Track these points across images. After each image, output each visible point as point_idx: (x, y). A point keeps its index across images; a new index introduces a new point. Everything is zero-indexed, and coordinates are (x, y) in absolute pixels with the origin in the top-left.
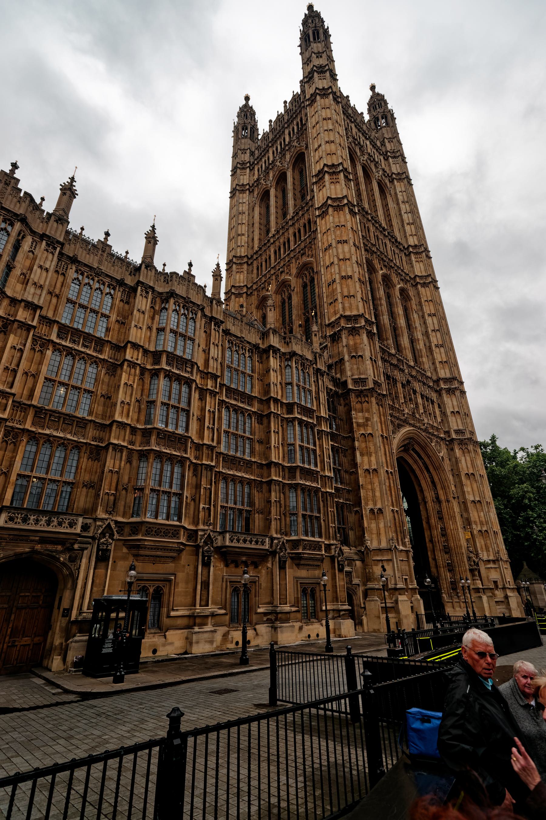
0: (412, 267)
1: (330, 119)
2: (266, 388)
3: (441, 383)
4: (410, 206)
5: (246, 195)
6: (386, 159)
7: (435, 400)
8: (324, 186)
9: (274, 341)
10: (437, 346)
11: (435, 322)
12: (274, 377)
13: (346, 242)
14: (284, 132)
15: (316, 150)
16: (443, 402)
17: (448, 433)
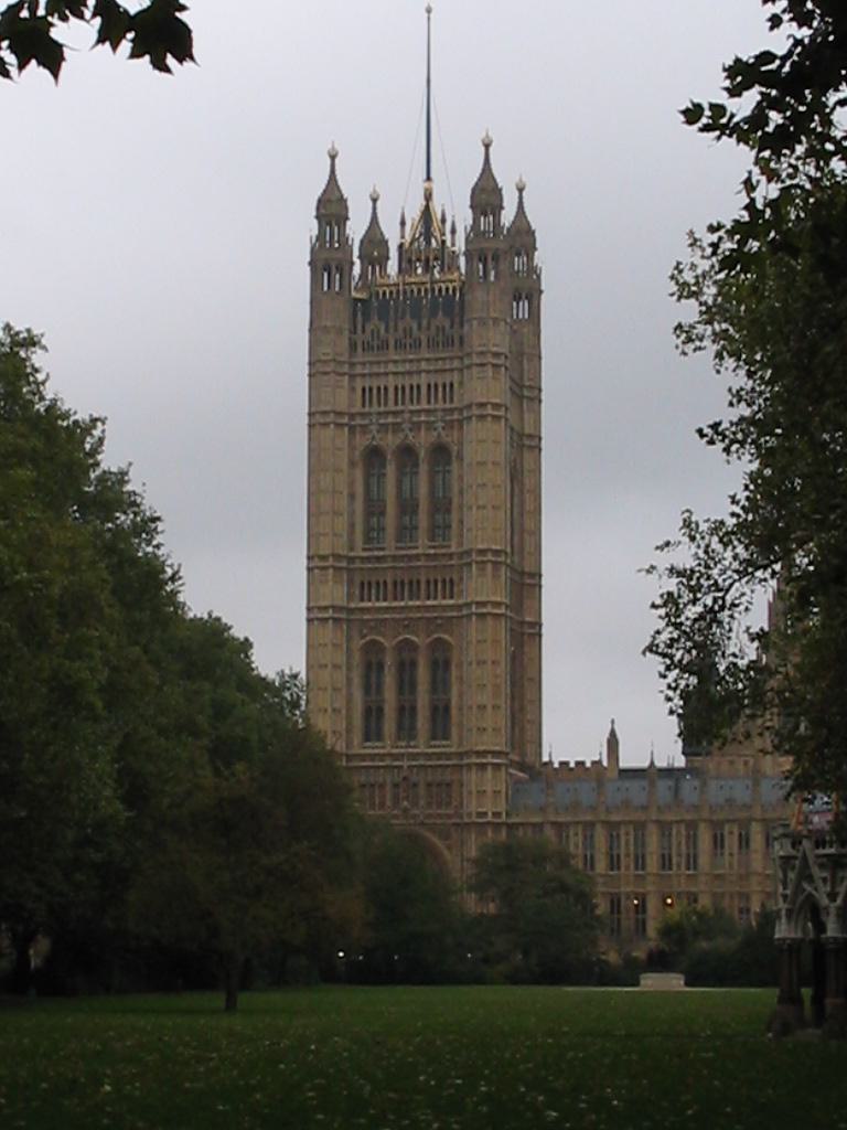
6: (521, 398)
14: (419, 372)
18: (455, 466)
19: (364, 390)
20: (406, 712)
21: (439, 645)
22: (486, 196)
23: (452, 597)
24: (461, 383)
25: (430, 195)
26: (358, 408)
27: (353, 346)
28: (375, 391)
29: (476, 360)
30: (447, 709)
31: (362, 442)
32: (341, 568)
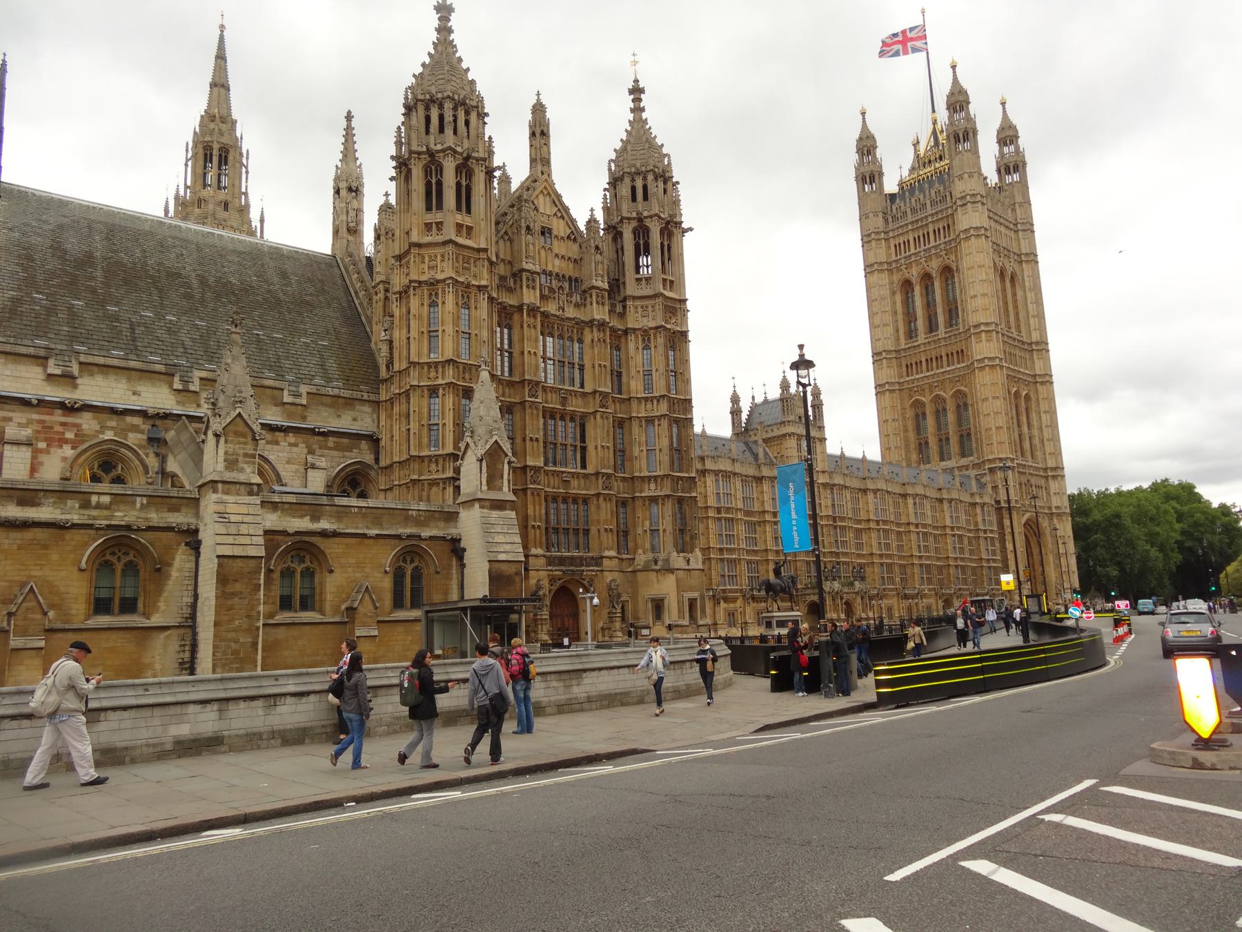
0: (1034, 363)
1: (983, 266)
2: (976, 524)
3: (1049, 471)
4: (1036, 295)
5: (885, 275)
6: (1016, 232)
7: (1044, 486)
8: (981, 341)
9: (978, 501)
10: (1048, 440)
11: (1048, 418)
12: (980, 519)
13: (998, 398)
14: (927, 225)
15: (972, 297)
16: (1049, 485)
17: (1050, 508)
18: (956, 274)
19: (895, 246)
20: (943, 441)
21: (959, 394)
22: (958, 101)
23: (963, 362)
24: (954, 223)
25: (936, 120)
26: (894, 258)
27: (886, 221)
28: (902, 245)
29: (959, 203)
30: (969, 435)
31: (896, 278)
32: (890, 358)
